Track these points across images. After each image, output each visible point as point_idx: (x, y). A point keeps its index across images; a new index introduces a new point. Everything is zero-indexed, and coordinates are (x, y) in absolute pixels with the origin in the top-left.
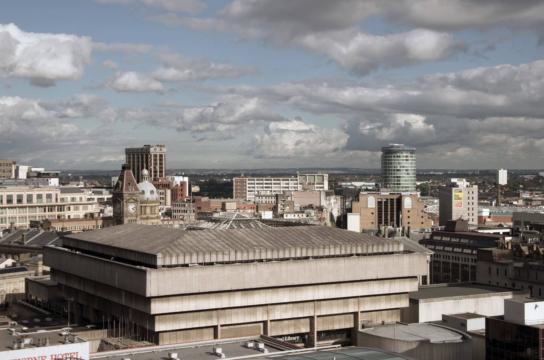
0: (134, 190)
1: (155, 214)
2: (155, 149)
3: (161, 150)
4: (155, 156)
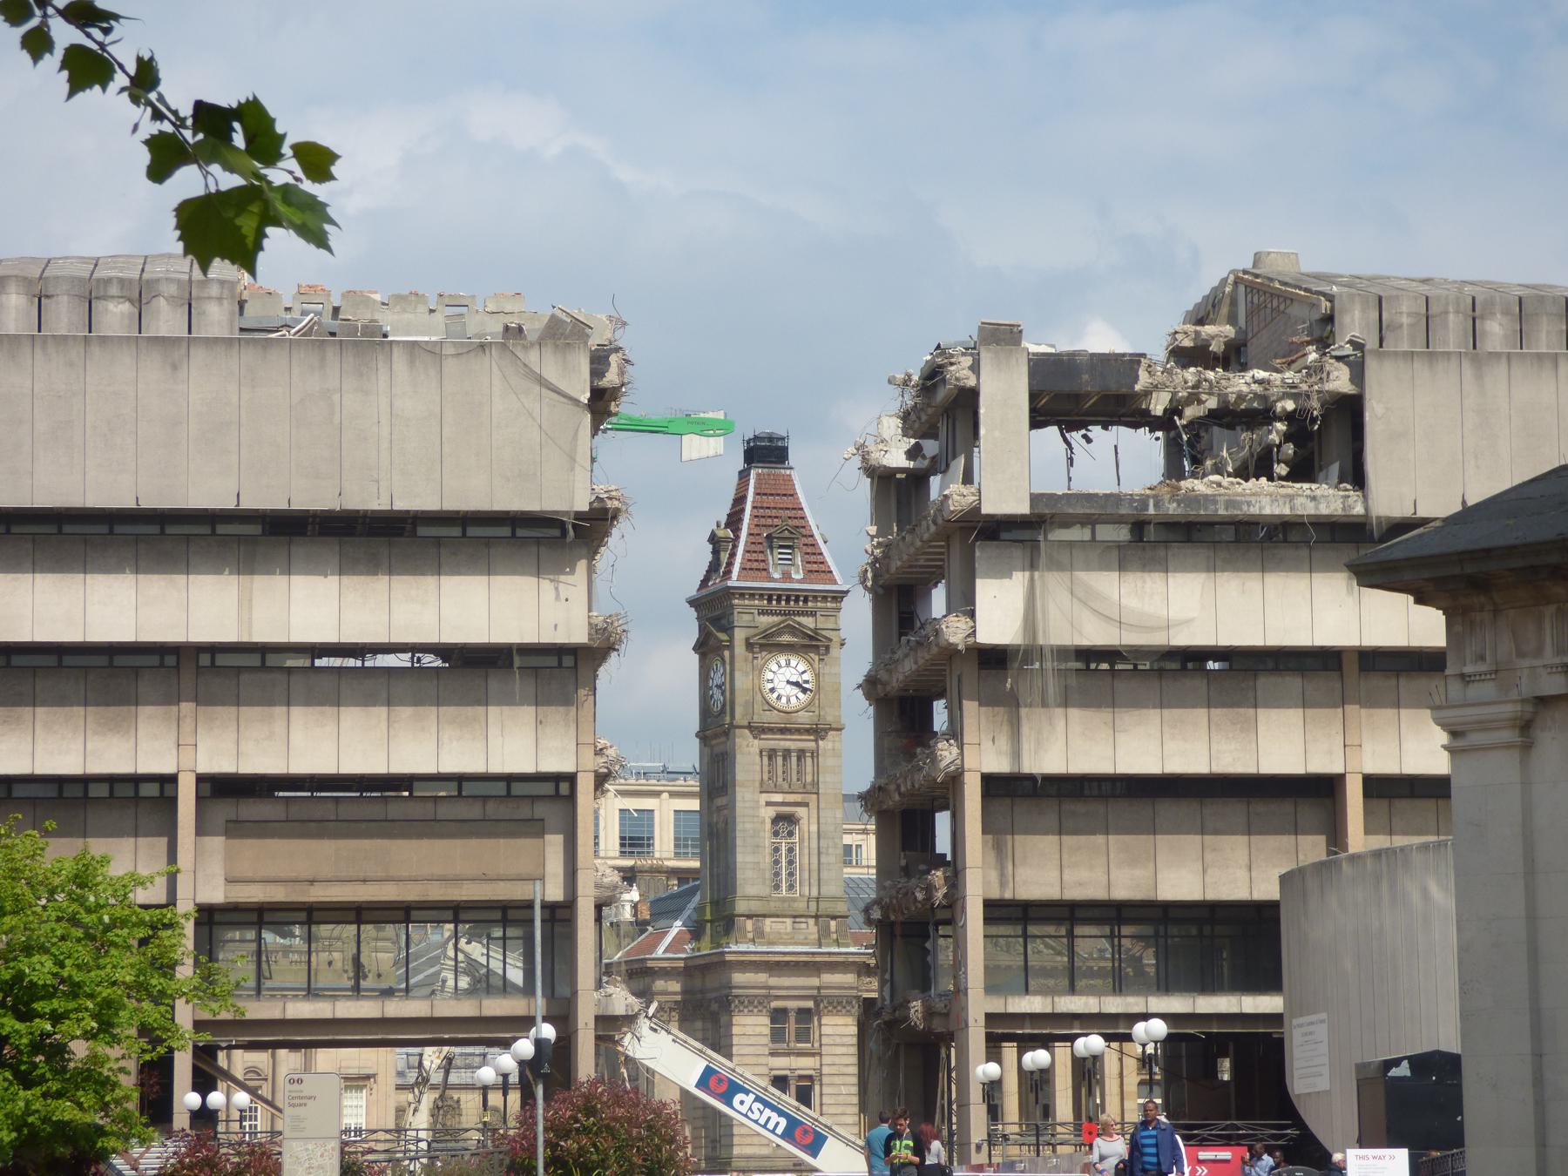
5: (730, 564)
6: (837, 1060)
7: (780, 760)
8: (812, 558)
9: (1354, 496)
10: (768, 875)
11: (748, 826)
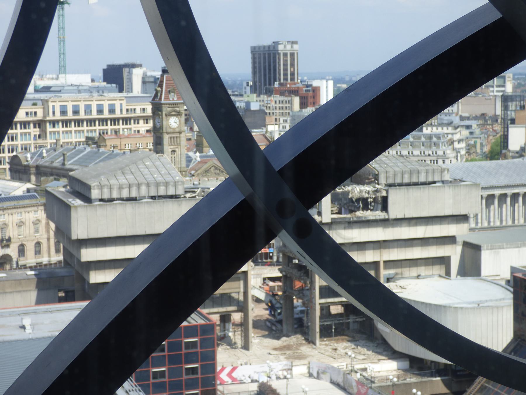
0: (175, 99)
2: (285, 47)
3: (292, 47)
4: (285, 55)
9: (385, 214)
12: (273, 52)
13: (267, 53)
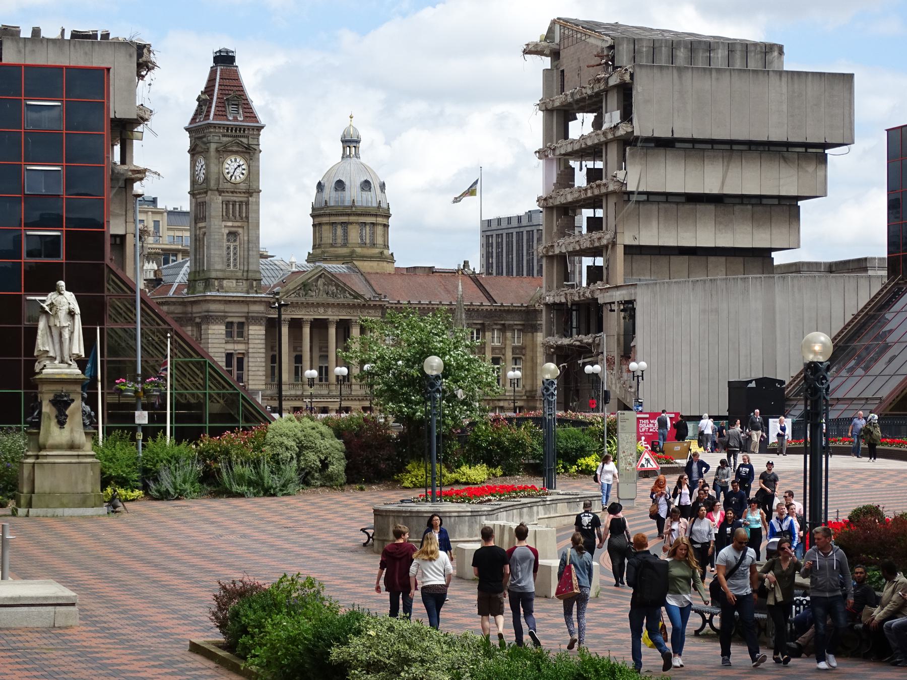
1: (374, 245)
5: (209, 112)
6: (256, 346)
7: (231, 206)
8: (247, 110)
10: (225, 260)
11: (216, 237)
12: (529, 229)
13: (514, 231)
